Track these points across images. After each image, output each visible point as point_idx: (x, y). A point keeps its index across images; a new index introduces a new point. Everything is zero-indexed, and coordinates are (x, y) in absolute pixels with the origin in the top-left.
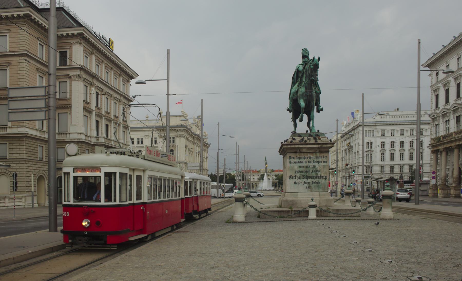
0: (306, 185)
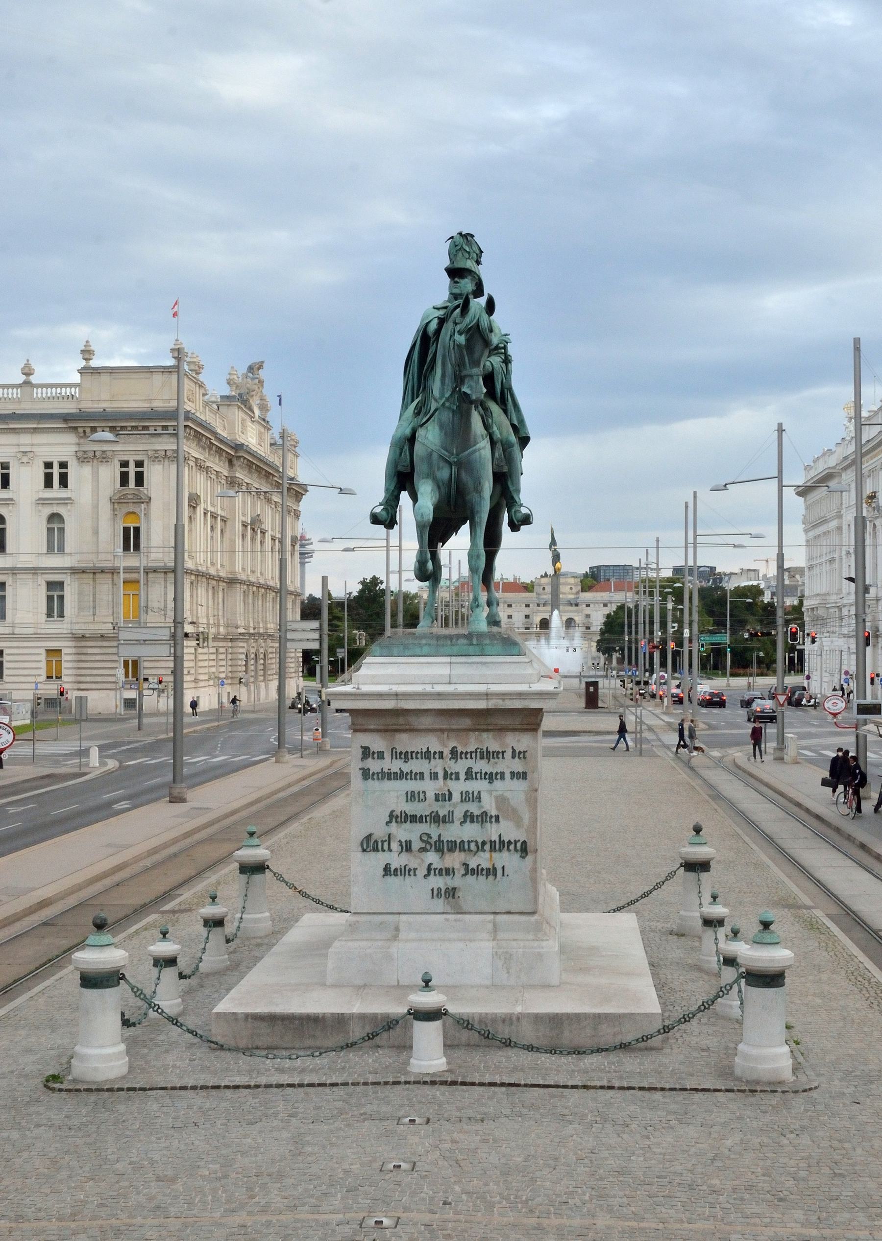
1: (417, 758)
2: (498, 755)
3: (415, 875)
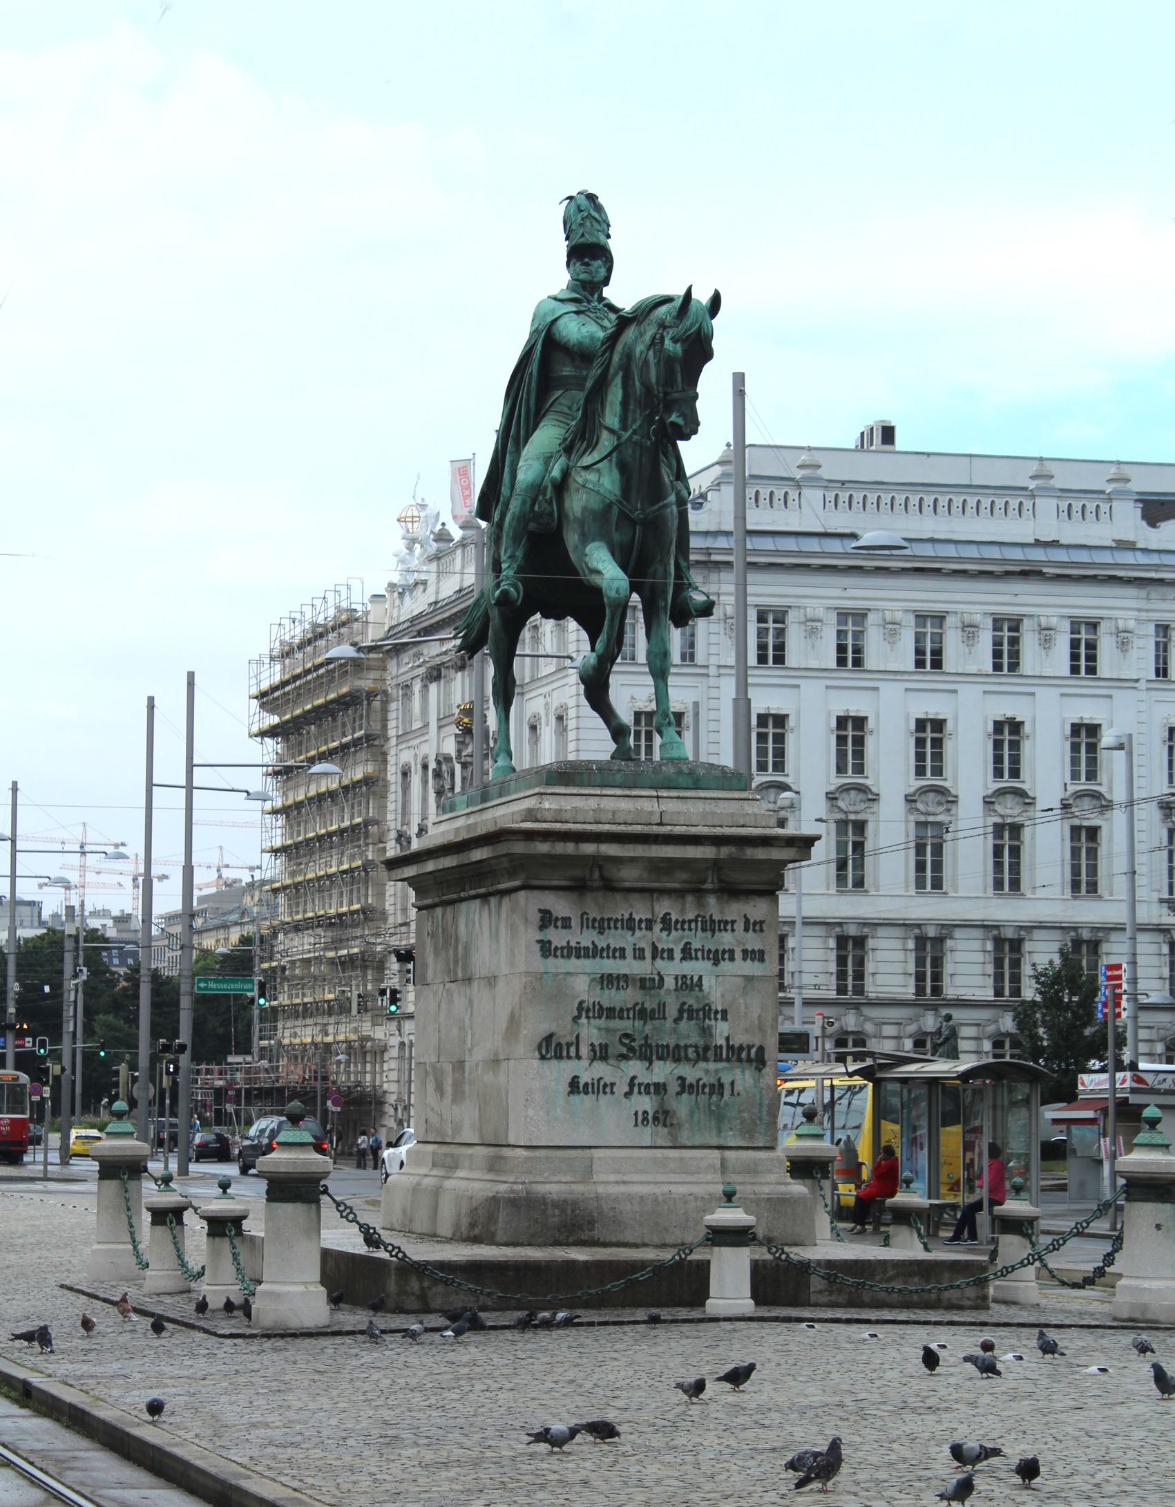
0: (646, 1103)
1: (616, 928)
2: (725, 925)
3: (612, 1093)
